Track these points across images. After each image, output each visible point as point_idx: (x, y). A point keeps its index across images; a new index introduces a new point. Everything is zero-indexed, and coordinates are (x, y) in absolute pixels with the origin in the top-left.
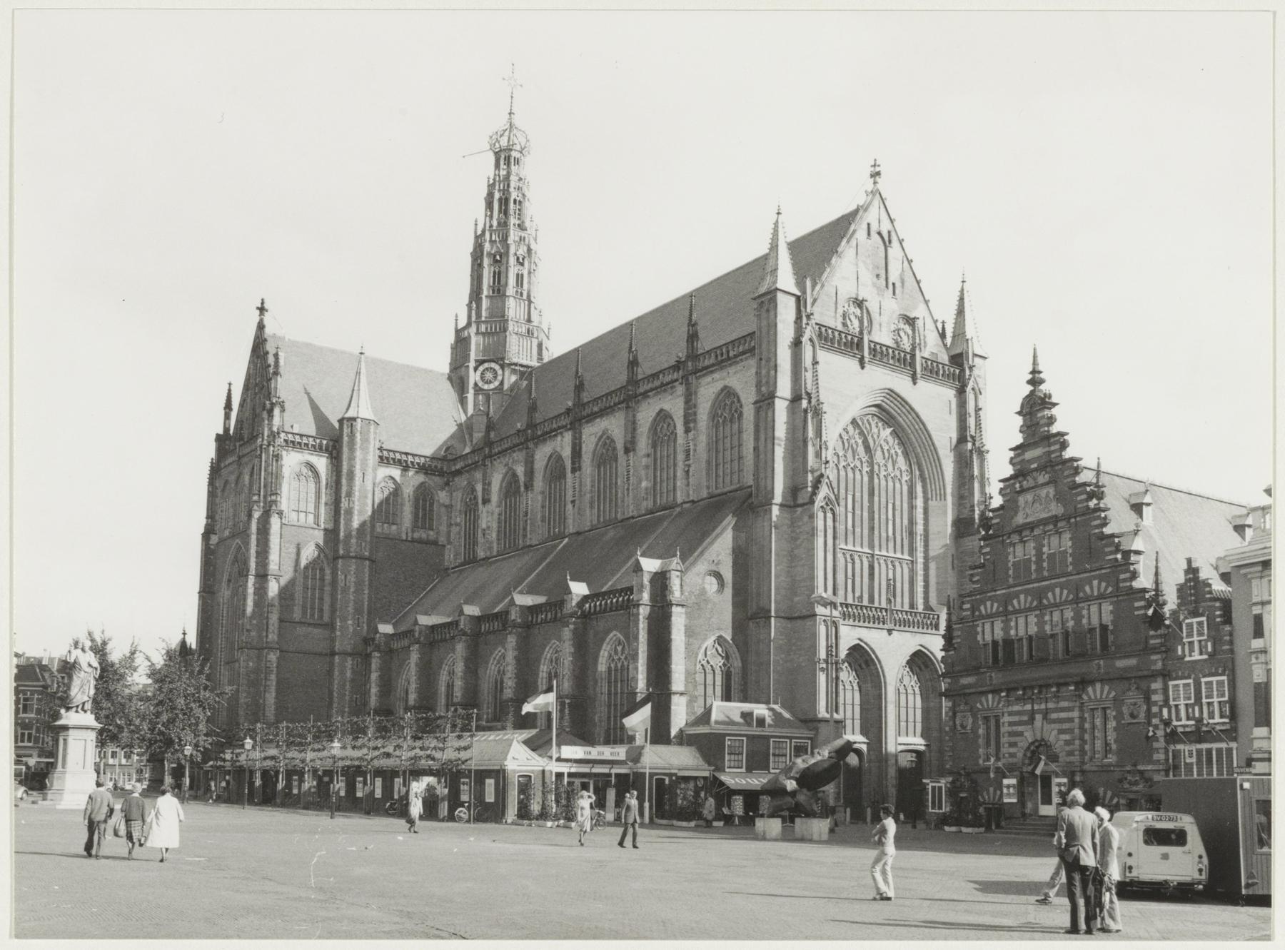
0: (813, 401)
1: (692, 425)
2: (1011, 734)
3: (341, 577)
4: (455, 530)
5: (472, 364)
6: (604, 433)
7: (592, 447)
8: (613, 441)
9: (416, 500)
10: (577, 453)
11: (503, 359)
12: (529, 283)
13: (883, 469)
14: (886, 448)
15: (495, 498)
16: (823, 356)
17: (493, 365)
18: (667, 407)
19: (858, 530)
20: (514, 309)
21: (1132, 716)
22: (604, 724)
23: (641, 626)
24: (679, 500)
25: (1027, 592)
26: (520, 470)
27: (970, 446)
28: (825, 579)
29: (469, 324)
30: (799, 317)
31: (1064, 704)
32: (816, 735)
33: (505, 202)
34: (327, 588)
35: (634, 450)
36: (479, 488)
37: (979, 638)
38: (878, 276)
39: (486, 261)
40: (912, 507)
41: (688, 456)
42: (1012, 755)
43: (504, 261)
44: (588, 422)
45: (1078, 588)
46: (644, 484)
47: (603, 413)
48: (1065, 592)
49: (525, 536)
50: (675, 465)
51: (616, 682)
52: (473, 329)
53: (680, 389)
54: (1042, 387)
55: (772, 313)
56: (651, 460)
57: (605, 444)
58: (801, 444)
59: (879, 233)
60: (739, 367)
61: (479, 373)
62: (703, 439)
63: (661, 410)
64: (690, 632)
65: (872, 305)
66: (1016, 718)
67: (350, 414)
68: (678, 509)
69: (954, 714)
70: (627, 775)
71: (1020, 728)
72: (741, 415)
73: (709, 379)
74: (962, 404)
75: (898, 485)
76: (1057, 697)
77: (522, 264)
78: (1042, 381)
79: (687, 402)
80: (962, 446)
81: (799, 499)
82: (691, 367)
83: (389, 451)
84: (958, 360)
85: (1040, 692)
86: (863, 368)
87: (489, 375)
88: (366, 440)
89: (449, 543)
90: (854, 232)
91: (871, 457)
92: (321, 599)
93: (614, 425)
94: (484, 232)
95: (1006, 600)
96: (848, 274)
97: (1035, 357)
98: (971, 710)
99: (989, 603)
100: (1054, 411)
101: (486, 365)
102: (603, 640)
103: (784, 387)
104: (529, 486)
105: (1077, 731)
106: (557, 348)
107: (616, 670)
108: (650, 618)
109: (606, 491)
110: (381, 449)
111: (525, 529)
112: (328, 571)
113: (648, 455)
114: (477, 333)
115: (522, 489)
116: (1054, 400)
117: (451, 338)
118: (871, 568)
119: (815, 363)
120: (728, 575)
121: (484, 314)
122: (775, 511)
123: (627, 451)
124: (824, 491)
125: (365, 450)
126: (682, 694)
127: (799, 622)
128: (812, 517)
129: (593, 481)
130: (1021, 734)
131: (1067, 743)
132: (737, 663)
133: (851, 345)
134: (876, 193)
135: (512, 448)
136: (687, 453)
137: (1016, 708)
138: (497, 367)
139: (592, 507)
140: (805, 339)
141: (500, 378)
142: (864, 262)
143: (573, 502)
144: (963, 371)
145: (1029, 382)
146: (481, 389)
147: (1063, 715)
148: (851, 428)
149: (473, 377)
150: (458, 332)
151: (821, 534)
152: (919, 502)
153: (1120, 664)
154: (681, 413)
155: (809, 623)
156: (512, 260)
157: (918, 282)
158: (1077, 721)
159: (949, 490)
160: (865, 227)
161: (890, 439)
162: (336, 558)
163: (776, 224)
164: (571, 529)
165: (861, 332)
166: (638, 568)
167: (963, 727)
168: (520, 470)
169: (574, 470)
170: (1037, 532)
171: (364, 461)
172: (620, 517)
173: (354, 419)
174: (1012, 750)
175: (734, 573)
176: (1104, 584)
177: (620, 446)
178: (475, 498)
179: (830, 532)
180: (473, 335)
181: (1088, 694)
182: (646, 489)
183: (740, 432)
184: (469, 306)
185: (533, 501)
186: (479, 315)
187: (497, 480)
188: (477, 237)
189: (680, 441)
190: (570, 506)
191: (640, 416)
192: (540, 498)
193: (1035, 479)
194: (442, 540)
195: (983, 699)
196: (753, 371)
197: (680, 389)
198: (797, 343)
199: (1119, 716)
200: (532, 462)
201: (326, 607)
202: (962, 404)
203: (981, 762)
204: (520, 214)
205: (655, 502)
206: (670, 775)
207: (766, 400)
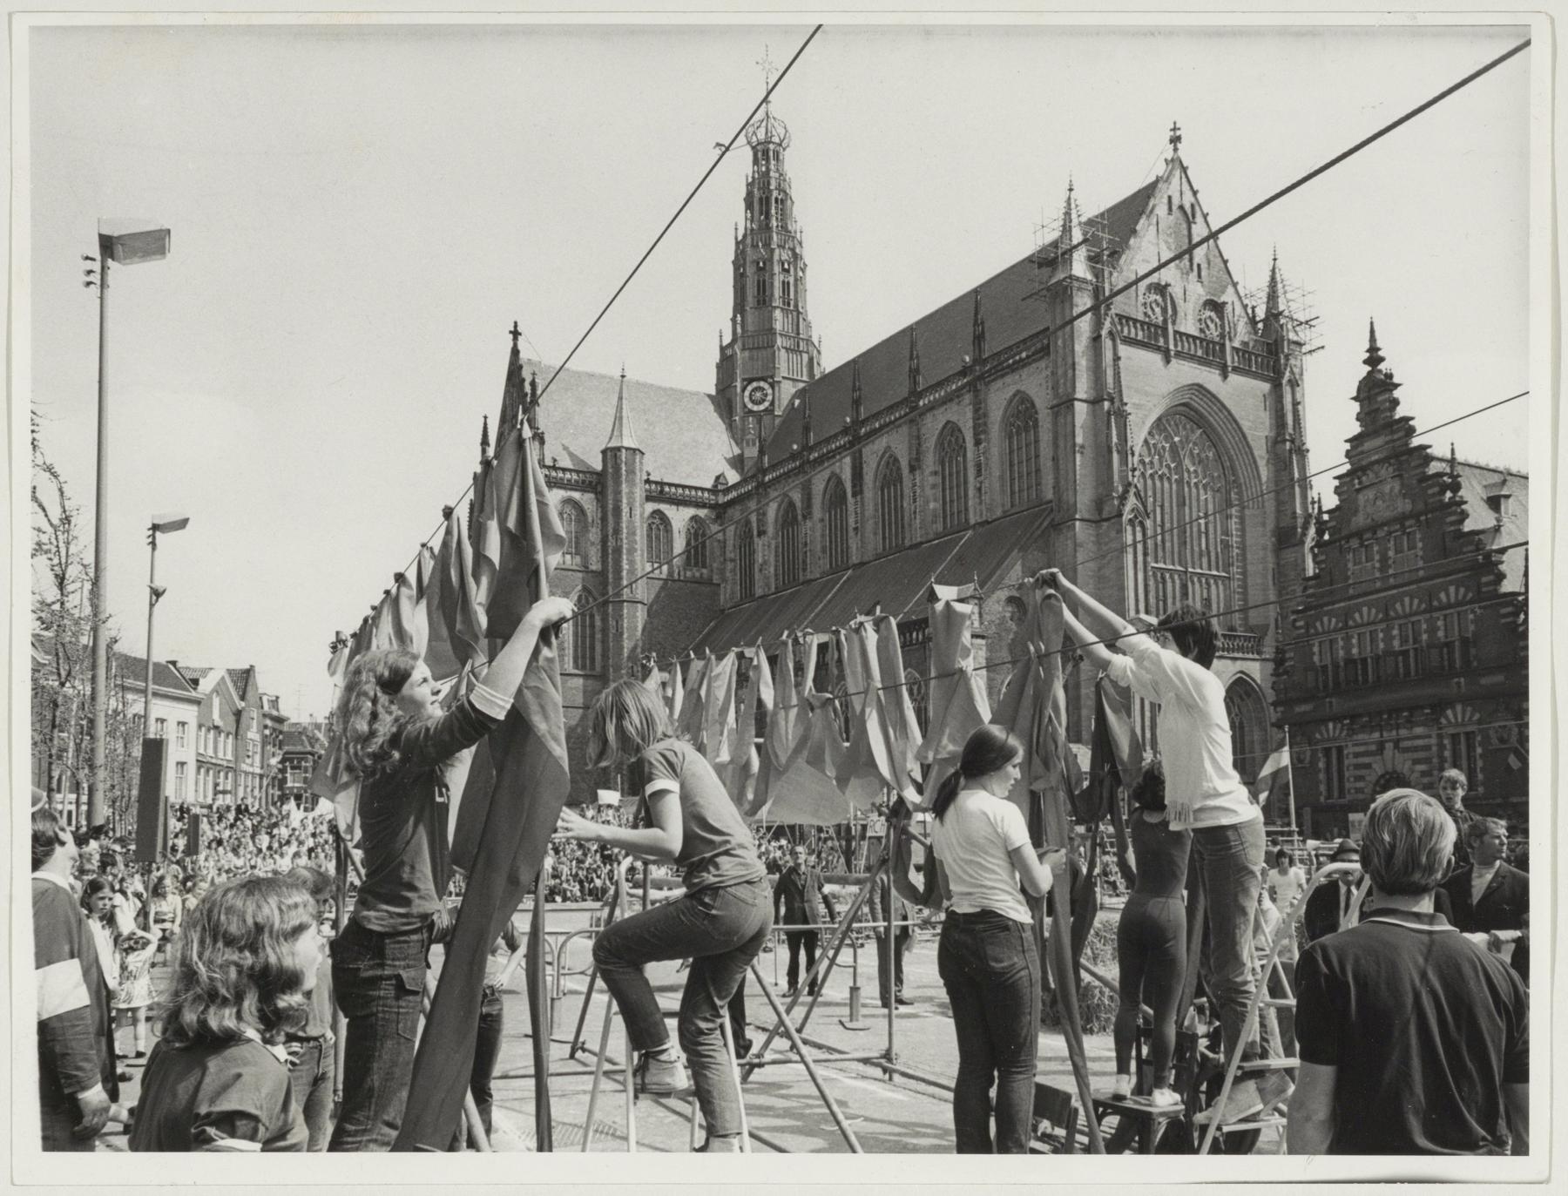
2: (1357, 767)
3: (612, 622)
4: (730, 566)
5: (738, 384)
8: (896, 460)
11: (772, 377)
15: (771, 530)
16: (1123, 350)
17: (762, 384)
18: (954, 419)
19: (1168, 544)
20: (779, 321)
21: (1502, 740)
24: (972, 522)
25: (1370, 605)
26: (797, 497)
28: (1137, 600)
29: (734, 340)
31: (1419, 730)
33: (765, 201)
34: (598, 636)
37: (1316, 658)
42: (1358, 790)
45: (1431, 595)
46: (932, 505)
48: (1416, 601)
49: (804, 570)
50: (966, 482)
52: (737, 348)
53: (968, 398)
54: (1382, 366)
59: (1181, 207)
62: (995, 451)
63: (948, 422)
65: (1176, 291)
66: (1362, 749)
68: (970, 533)
71: (1366, 760)
72: (1036, 426)
73: (999, 383)
76: (1410, 723)
77: (788, 271)
78: (1382, 359)
79: (976, 411)
81: (1105, 515)
82: (982, 372)
85: (1390, 718)
87: (758, 394)
88: (631, 472)
89: (724, 580)
92: (593, 648)
93: (897, 442)
94: (745, 236)
95: (1347, 615)
97: (1372, 332)
99: (1326, 619)
100: (1396, 393)
101: (755, 384)
103: (1083, 389)
104: (807, 515)
105: (1435, 760)
106: (830, 361)
109: (893, 516)
110: (648, 481)
111: (804, 562)
112: (597, 618)
113: (936, 473)
114: (743, 349)
116: (1396, 380)
117: (716, 357)
119: (1117, 358)
123: (912, 469)
124: (1132, 501)
125: (632, 483)
128: (1120, 531)
130: (1368, 766)
131: (1423, 774)
133: (1154, 337)
134: (1177, 164)
136: (979, 467)
137: (1360, 737)
138: (766, 386)
140: (1104, 333)
141: (770, 398)
143: (856, 529)
145: (1365, 362)
146: (751, 411)
147: (1420, 742)
150: (722, 349)
153: (1483, 681)
154: (970, 423)
156: (777, 269)
157: (1225, 262)
158: (1434, 749)
160: (1165, 200)
162: (606, 603)
164: (855, 559)
165: (1165, 321)
166: (933, 598)
168: (797, 497)
169: (854, 495)
170: (1381, 534)
171: (631, 494)
172: (907, 543)
173: (619, 449)
174: (1360, 784)
176: (1462, 590)
177: (904, 463)
178: (750, 530)
181: (1447, 718)
182: (935, 510)
183: (1037, 441)
184: (734, 320)
185: (814, 530)
187: (772, 511)
188: (737, 243)
189: (970, 455)
190: (851, 533)
193: (1377, 474)
194: (716, 579)
197: (968, 398)
199: (1486, 740)
201: (598, 657)
203: (1322, 799)
207: (1064, 405)
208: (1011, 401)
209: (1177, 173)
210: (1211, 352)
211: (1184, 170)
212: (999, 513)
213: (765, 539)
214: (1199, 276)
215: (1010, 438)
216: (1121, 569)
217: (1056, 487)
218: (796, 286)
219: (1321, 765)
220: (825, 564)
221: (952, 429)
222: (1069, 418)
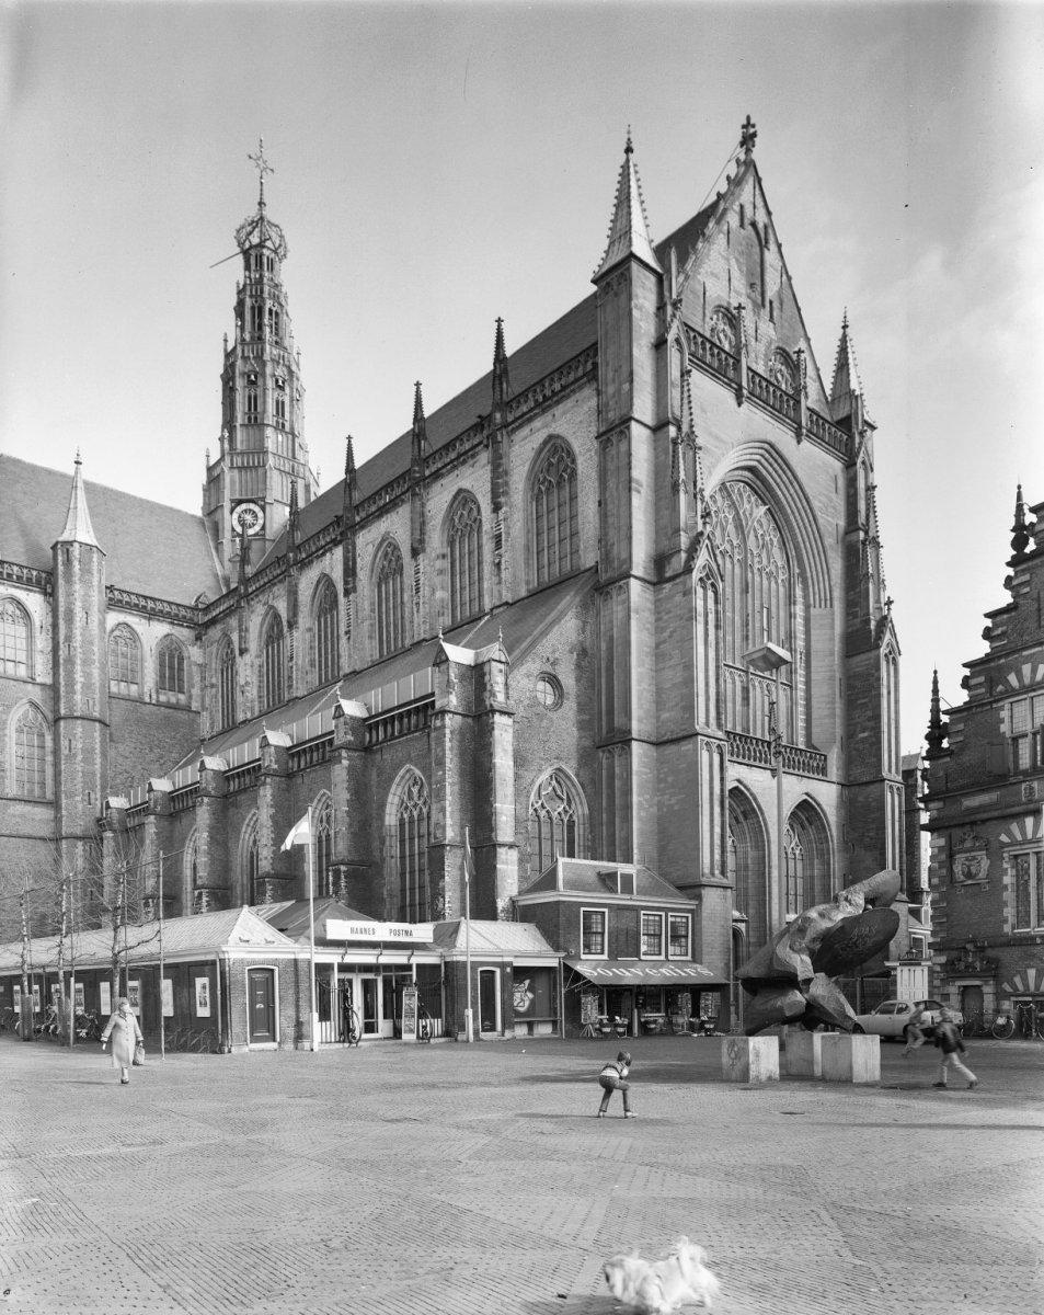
0: (685, 428)
1: (502, 499)
6: (383, 540)
7: (368, 559)
8: (396, 548)
9: (161, 655)
10: (350, 571)
11: (263, 499)
12: (291, 413)
13: (757, 559)
14: (761, 532)
22: (397, 900)
23: (448, 745)
24: (487, 608)
27: (862, 535)
28: (707, 684)
29: (222, 458)
30: (661, 308)
32: (699, 905)
35: (424, 550)
36: (235, 637)
38: (752, 285)
39: (240, 383)
40: (791, 616)
41: (498, 545)
43: (260, 382)
44: (363, 528)
46: (439, 594)
47: (383, 511)
49: (290, 687)
51: (412, 839)
55: (623, 297)
56: (446, 564)
57: (386, 554)
58: (669, 489)
60: (569, 403)
61: (235, 516)
64: (520, 760)
67: (65, 537)
69: (951, 857)
70: (436, 967)
72: (573, 475)
73: (525, 431)
74: (851, 482)
75: (773, 585)
80: (852, 537)
83: (121, 591)
84: (846, 423)
86: (739, 405)
88: (86, 571)
90: (725, 210)
91: (744, 541)
96: (717, 274)
98: (987, 847)
102: (391, 780)
107: (411, 822)
108: (461, 733)
111: (290, 678)
113: (444, 556)
114: (232, 468)
115: (285, 629)
118: (746, 690)
120: (568, 680)
121: (239, 446)
122: (635, 585)
123: (415, 553)
124: (703, 557)
126: (511, 846)
127: (672, 748)
128: (688, 593)
129: (372, 604)
132: (581, 810)
133: (725, 366)
135: (272, 583)
139: (370, 637)
140: (671, 337)
142: (737, 260)
144: (851, 437)
148: (718, 497)
149: (230, 521)
150: (210, 469)
151: (701, 619)
152: (799, 609)
155: (686, 747)
159: (838, 593)
160: (737, 208)
161: (764, 521)
163: (626, 167)
164: (346, 670)
167: (969, 875)
169: (347, 593)
172: (408, 642)
175: (578, 680)
179: (711, 617)
180: (226, 469)
182: (442, 600)
186: (232, 447)
187: (255, 620)
190: (343, 640)
191: (430, 506)
192: (308, 635)
195: (1014, 827)
196: (593, 402)
198: (660, 345)
200: (296, 593)
202: (851, 482)
204: (277, 329)
205: (453, 616)
206: (502, 965)
207: (614, 431)
208: (540, 451)
209: (751, 179)
210: (780, 398)
211: (759, 180)
212: (523, 593)
213: (248, 658)
214: (771, 316)
215: (538, 498)
216: (689, 639)
217: (603, 540)
218: (292, 406)
219: (1008, 880)
220: (313, 678)
221: (464, 498)
222: (623, 447)
